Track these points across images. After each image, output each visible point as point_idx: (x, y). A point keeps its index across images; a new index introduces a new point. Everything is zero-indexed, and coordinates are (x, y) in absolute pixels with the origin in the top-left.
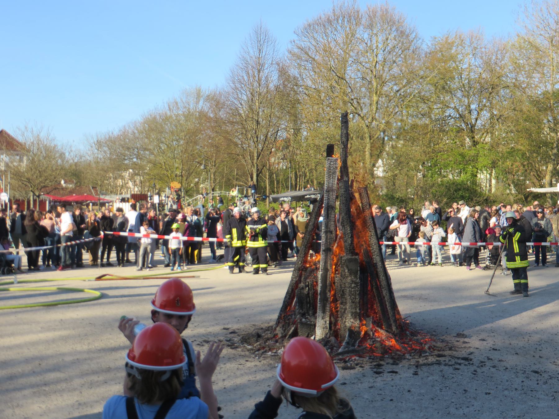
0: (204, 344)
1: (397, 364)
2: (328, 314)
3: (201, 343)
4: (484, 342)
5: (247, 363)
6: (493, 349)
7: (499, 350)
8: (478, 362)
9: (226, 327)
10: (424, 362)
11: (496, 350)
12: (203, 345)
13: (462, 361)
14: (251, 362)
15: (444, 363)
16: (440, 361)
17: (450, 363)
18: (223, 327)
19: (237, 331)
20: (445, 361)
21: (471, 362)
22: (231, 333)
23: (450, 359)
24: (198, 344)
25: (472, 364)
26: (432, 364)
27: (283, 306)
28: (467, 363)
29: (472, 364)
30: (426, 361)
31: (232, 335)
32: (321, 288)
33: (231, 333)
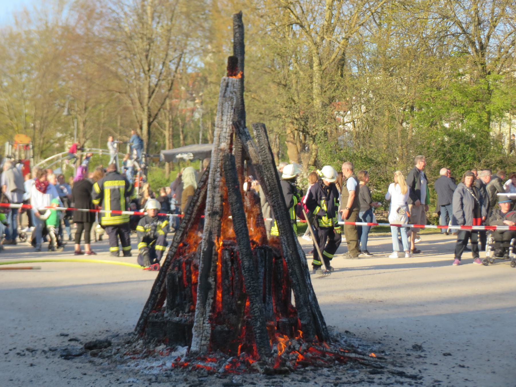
0: (27, 353)
1: (308, 381)
2: (208, 309)
3: (23, 351)
4: (449, 356)
5: (85, 376)
6: (460, 366)
7: (468, 367)
8: (432, 381)
9: (65, 332)
10: (349, 379)
11: (463, 367)
12: (24, 355)
13: (408, 380)
14: (91, 375)
15: (379, 381)
16: (373, 379)
17: (389, 381)
18: (59, 334)
19: (80, 338)
20: (381, 379)
21: (419, 381)
22: (71, 340)
23: (390, 376)
24: (18, 354)
25: (421, 383)
26: (361, 381)
27: (149, 299)
28: (413, 382)
29: (421, 383)
30: (353, 378)
31: (73, 343)
32: (202, 270)
33: (71, 340)
